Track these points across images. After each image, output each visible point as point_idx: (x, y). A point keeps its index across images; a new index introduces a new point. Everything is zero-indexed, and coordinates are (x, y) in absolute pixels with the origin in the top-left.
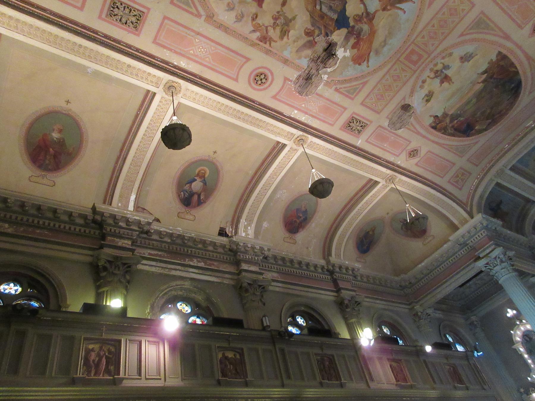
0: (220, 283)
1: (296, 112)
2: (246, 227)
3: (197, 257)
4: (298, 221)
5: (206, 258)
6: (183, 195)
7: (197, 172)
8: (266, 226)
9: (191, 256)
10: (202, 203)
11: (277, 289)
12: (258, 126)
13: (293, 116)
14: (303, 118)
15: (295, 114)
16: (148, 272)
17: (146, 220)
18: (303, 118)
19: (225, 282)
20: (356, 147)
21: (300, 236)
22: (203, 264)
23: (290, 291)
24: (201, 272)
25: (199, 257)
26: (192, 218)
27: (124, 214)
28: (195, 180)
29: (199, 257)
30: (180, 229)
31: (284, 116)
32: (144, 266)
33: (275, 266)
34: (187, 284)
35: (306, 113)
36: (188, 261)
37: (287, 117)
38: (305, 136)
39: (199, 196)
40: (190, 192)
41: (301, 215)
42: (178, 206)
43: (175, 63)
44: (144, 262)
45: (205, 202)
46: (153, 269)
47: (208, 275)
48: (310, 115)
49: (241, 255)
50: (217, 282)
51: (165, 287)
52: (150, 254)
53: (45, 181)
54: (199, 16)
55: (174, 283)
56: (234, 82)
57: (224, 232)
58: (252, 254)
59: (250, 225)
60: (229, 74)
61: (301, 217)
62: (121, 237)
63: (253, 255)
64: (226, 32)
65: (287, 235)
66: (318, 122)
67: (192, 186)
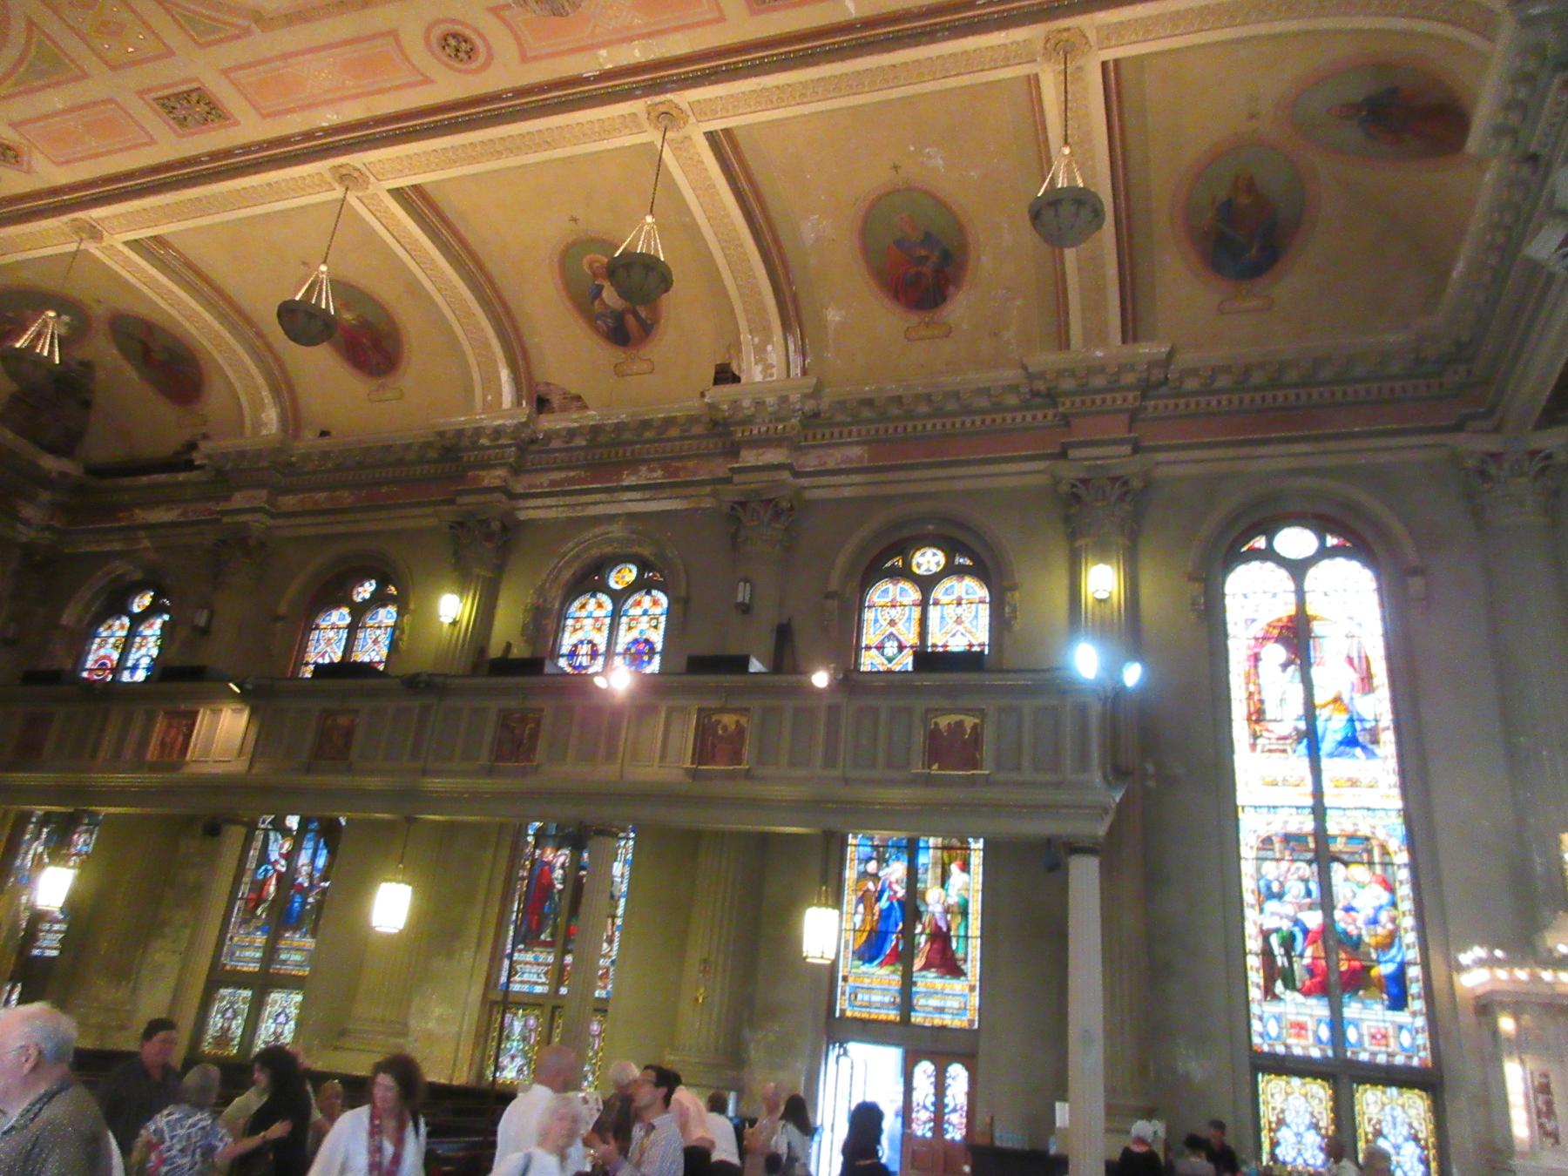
0: (695, 510)
1: (603, 53)
2: (760, 351)
3: (645, 461)
4: (927, 269)
5: (666, 458)
6: (603, 325)
7: (586, 268)
8: (837, 318)
9: (632, 464)
10: (652, 326)
11: (847, 492)
12: (547, 145)
13: (609, 66)
14: (636, 54)
15: (607, 59)
16: (545, 521)
17: (515, 421)
18: (637, 53)
19: (703, 505)
20: (848, 27)
21: (959, 308)
22: (660, 473)
23: (889, 490)
24: (647, 495)
25: (653, 460)
26: (645, 366)
27: (476, 421)
28: (600, 288)
29: (653, 460)
30: (594, 413)
31: (586, 81)
32: (531, 511)
33: (854, 429)
34: (617, 530)
35: (630, 40)
36: (627, 475)
37: (598, 79)
38: (661, 103)
39: (636, 315)
40: (612, 312)
41: (923, 253)
42: (607, 354)
43: (325, 124)
44: (532, 503)
45: (655, 322)
46: (552, 513)
47: (665, 498)
48: (641, 36)
49: (739, 429)
50: (686, 510)
51: (571, 545)
52: (553, 483)
53: (389, 395)
54: (247, 32)
55: (588, 535)
56: (426, 89)
57: (729, 375)
58: (767, 420)
59: (767, 340)
60: (398, 82)
61: (926, 258)
62: (487, 465)
63: (770, 421)
64: (306, 20)
65: (914, 318)
66: (678, 36)
67: (606, 301)
